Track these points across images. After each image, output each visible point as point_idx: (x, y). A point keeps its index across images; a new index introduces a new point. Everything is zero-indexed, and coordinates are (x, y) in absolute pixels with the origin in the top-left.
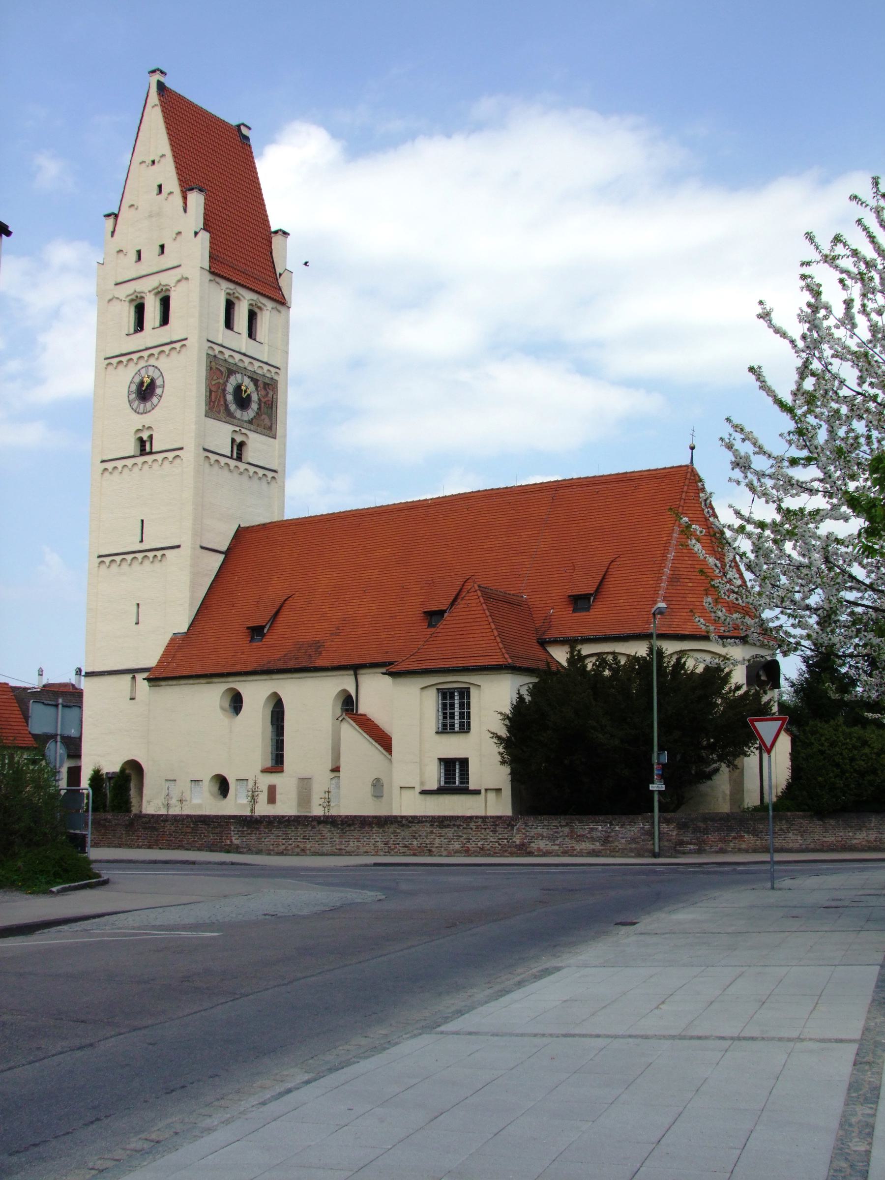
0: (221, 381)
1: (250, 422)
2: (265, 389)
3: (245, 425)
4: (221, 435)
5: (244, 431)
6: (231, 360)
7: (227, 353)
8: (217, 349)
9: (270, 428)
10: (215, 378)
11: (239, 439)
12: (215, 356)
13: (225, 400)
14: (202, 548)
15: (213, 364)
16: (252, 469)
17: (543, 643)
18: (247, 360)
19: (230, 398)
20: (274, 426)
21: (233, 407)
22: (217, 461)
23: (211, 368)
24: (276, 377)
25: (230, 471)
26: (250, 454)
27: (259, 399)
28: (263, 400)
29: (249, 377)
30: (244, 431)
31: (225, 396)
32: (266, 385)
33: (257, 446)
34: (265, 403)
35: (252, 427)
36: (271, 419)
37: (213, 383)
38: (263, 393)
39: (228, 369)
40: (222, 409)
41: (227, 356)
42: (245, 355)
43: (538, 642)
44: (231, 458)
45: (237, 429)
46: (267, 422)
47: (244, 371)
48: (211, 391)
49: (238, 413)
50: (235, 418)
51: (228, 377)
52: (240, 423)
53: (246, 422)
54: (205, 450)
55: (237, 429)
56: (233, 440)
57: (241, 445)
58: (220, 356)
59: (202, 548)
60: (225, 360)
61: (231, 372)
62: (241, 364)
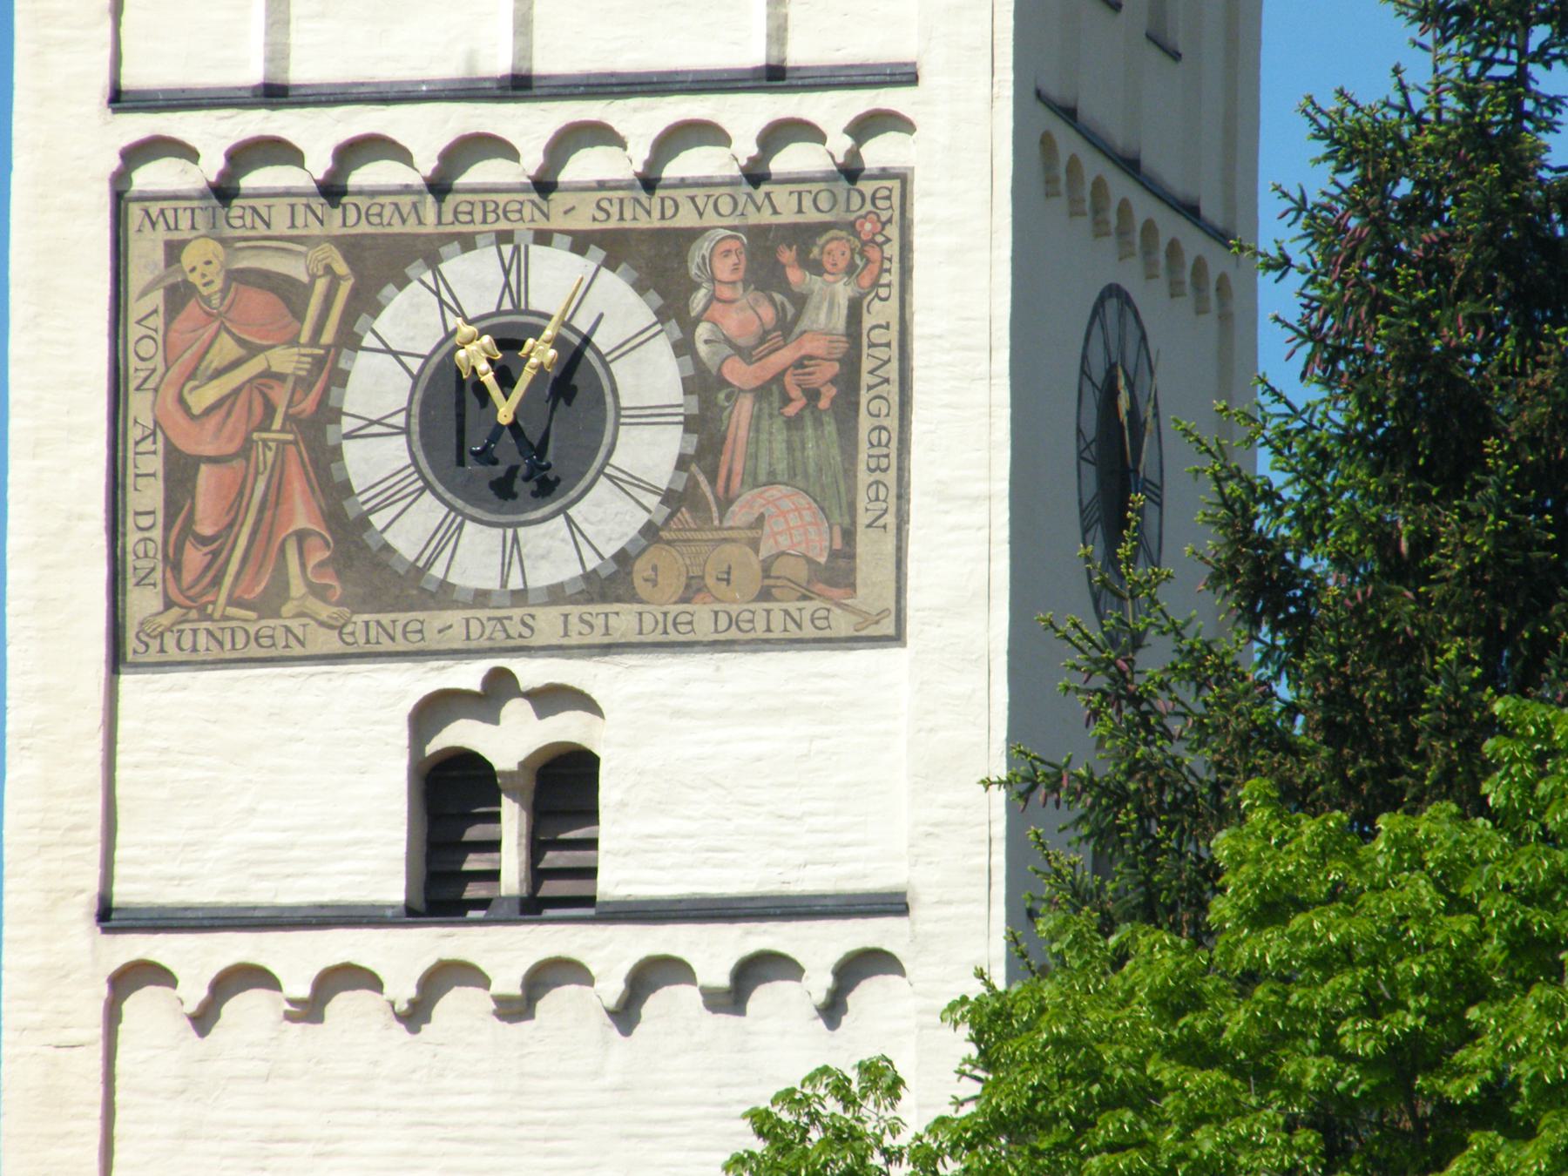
0: (284, 360)
5: (531, 672)
9: (838, 571)
10: (226, 348)
13: (333, 489)
19: (376, 460)
21: (411, 526)
23: (178, 296)
27: (703, 384)
28: (739, 373)
35: (623, 620)
38: (744, 315)
45: (469, 676)
46: (795, 528)
49: (477, 555)
50: (445, 596)
51: (365, 302)
53: (556, 595)
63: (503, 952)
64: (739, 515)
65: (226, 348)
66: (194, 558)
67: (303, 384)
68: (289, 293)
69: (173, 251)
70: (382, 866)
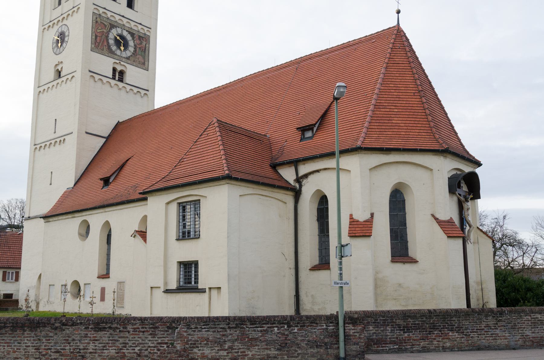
0: (105, 31)
1: (128, 58)
2: (140, 40)
3: (124, 60)
4: (105, 64)
6: (112, 19)
7: (109, 14)
8: (101, 10)
9: (144, 64)
11: (119, 68)
12: (100, 15)
13: (108, 43)
14: (87, 133)
15: (98, 19)
16: (129, 88)
17: (274, 167)
18: (125, 21)
19: (111, 42)
20: (146, 63)
22: (100, 79)
23: (97, 22)
24: (148, 33)
25: (111, 86)
26: (128, 78)
27: (135, 45)
28: (138, 46)
29: (127, 31)
30: (122, 63)
31: (107, 40)
32: (140, 37)
33: (133, 73)
34: (140, 48)
35: (129, 62)
36: (144, 58)
37: (99, 31)
38: (138, 42)
39: (110, 24)
40: (105, 48)
41: (109, 16)
42: (123, 16)
43: (271, 166)
44: (114, 78)
46: (141, 59)
47: (123, 27)
48: (96, 36)
50: (116, 54)
51: (111, 29)
52: (120, 58)
53: (124, 58)
54: (90, 71)
55: (118, 62)
56: (114, 70)
57: (122, 73)
58: (103, 15)
59: (87, 133)
60: (108, 18)
61: (113, 26)
62: (120, 22)
63: (121, 84)
64: (138, 57)
65: (100, 28)
66: (97, 44)
67: (106, 33)
68: (105, 26)
69: (96, 18)
70: (110, 75)
